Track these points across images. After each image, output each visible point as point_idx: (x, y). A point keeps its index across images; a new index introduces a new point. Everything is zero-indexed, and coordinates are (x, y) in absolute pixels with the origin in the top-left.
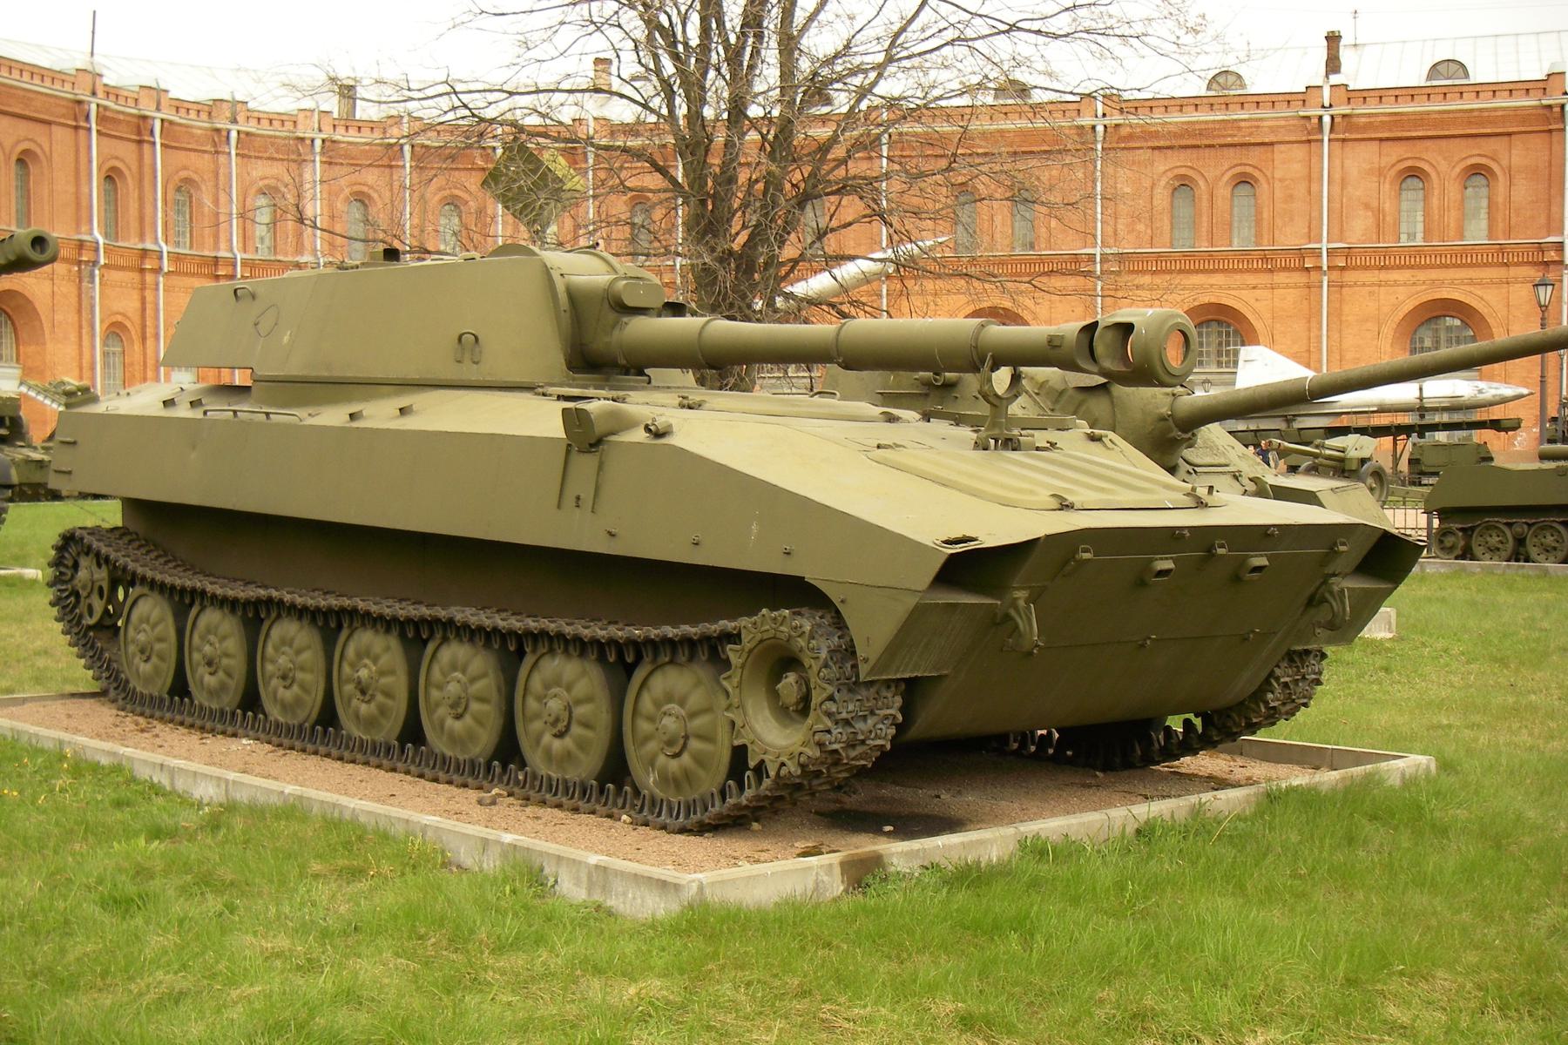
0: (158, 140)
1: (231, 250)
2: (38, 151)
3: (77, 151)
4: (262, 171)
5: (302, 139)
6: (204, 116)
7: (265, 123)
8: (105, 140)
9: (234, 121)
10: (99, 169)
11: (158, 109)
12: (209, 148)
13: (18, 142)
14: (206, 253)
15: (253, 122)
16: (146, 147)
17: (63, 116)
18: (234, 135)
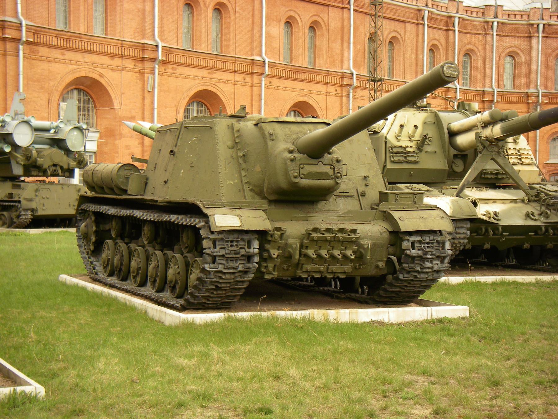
0: (457, 29)
1: (492, 87)
2: (399, 37)
3: (417, 36)
4: (508, 43)
5: (532, 25)
6: (480, 15)
7: (512, 17)
8: (431, 29)
9: (496, 16)
10: (428, 44)
11: (457, 12)
12: (481, 32)
13: (389, 33)
14: (479, 89)
15: (506, 17)
16: (450, 32)
17: (412, 18)
18: (495, 24)
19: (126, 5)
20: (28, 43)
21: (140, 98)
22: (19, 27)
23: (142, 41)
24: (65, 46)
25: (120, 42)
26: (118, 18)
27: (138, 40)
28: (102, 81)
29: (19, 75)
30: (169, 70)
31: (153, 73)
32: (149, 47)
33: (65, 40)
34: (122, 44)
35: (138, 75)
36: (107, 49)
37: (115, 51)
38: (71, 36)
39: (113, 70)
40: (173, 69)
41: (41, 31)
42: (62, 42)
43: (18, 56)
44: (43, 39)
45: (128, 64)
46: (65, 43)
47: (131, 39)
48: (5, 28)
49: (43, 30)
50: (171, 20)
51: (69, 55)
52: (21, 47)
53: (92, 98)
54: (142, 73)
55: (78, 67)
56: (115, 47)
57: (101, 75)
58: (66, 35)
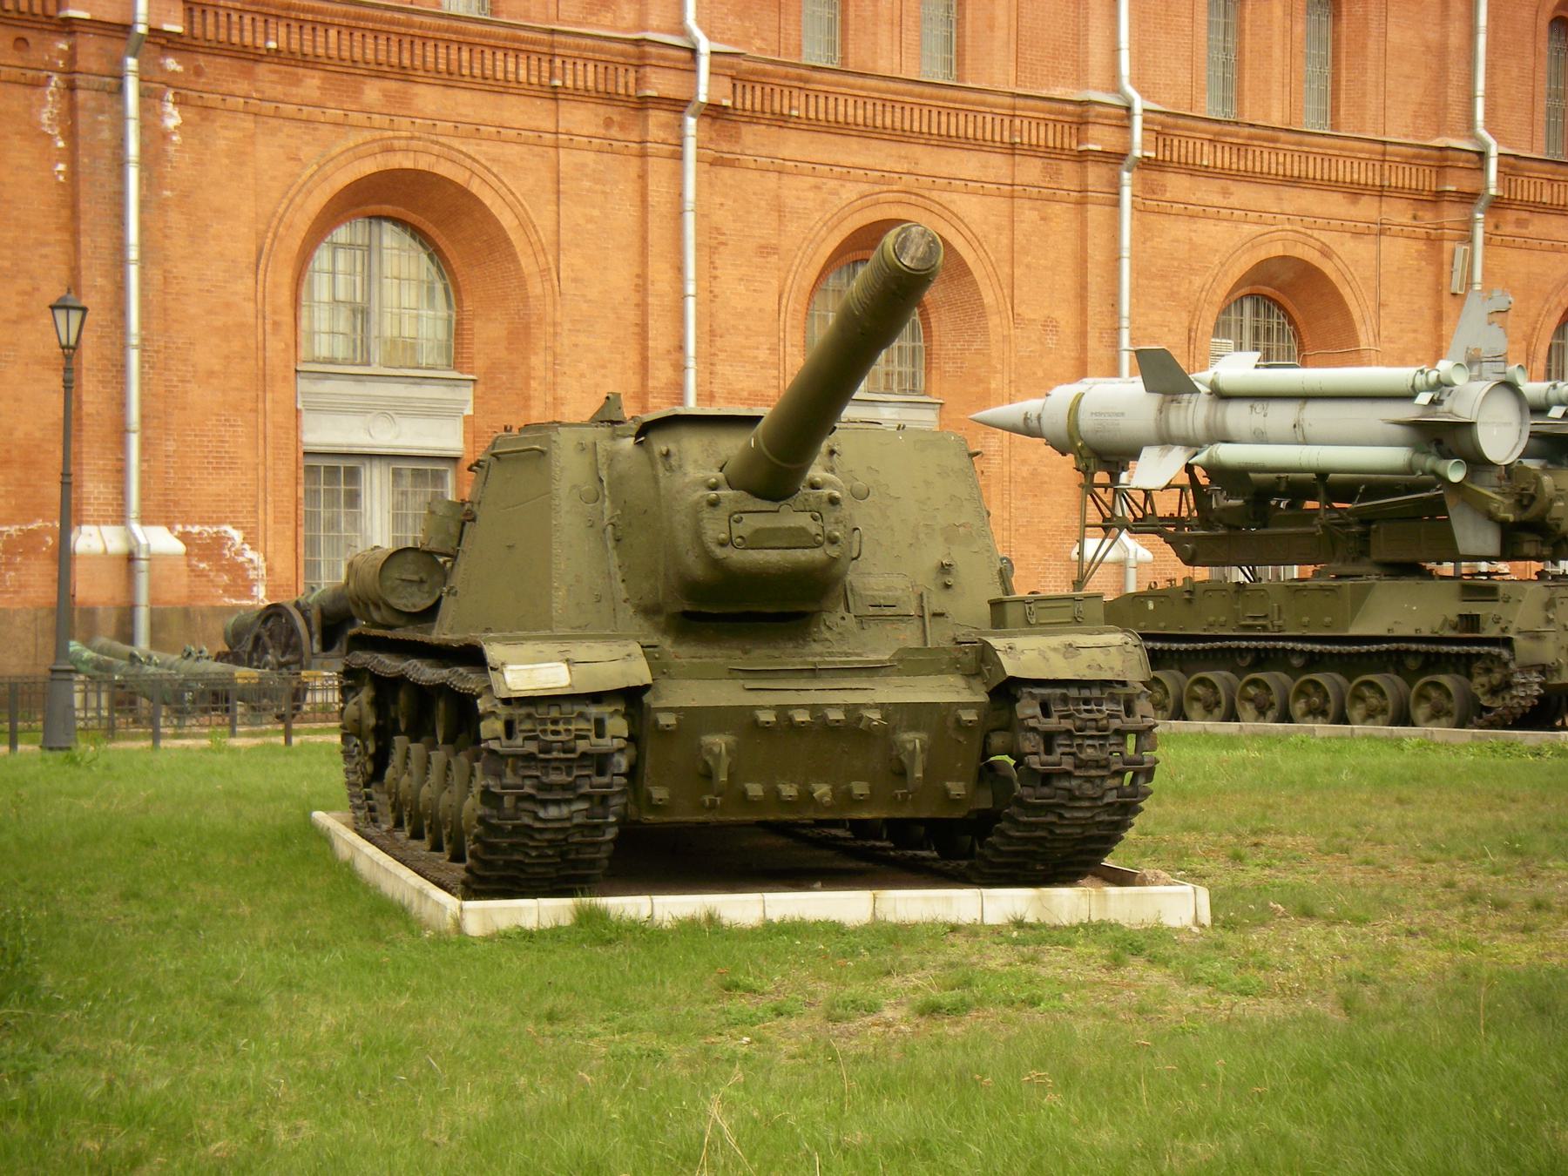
19: (1394, 36)
20: (1145, 164)
21: (1428, 315)
22: (1121, 118)
23: (1439, 142)
24: (1234, 166)
25: (1379, 147)
26: (1371, 76)
27: (1424, 138)
28: (1328, 268)
29: (1118, 259)
30: (1509, 229)
31: (1469, 240)
32: (1458, 160)
33: (1235, 151)
34: (1384, 154)
35: (1421, 246)
36: (1345, 171)
37: (1363, 174)
38: (1251, 137)
39: (1357, 234)
40: (1520, 223)
41: (1176, 127)
42: (1227, 155)
43: (1117, 204)
44: (1179, 150)
45: (1398, 213)
46: (1235, 159)
47: (1406, 136)
48: (1087, 123)
49: (1181, 121)
50: (1515, 72)
51: (1243, 194)
52: (1126, 176)
53: (1291, 322)
54: (1434, 241)
55: (1266, 229)
56: (1363, 165)
57: (1326, 252)
58: (1237, 135)
